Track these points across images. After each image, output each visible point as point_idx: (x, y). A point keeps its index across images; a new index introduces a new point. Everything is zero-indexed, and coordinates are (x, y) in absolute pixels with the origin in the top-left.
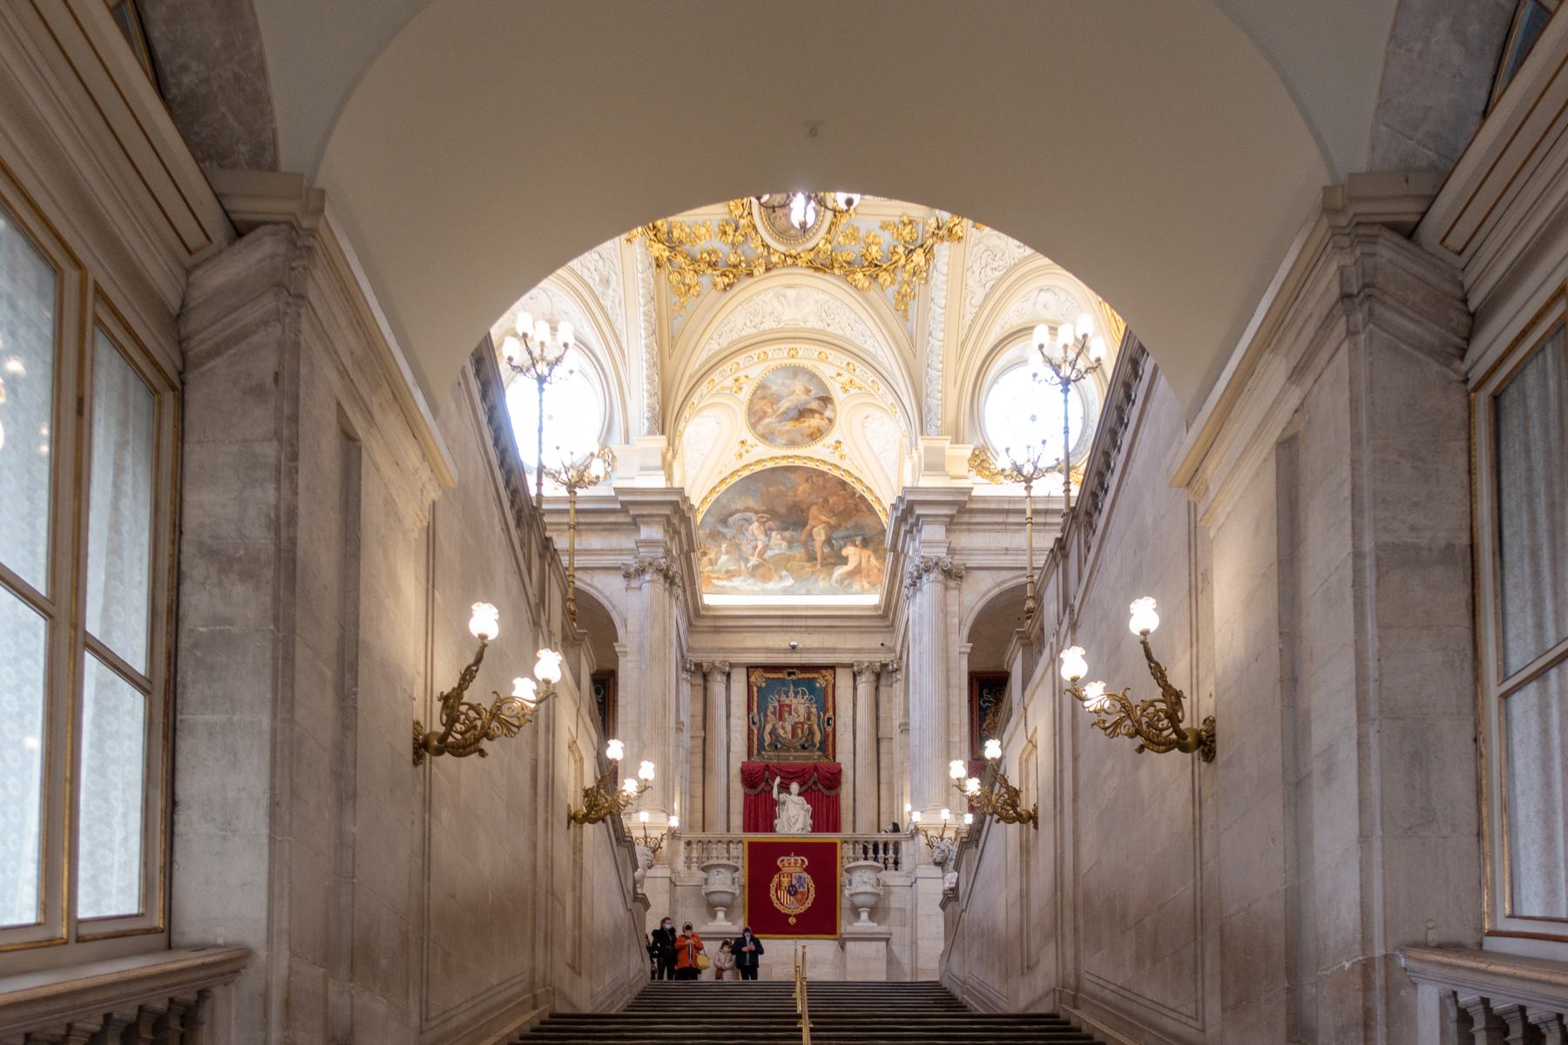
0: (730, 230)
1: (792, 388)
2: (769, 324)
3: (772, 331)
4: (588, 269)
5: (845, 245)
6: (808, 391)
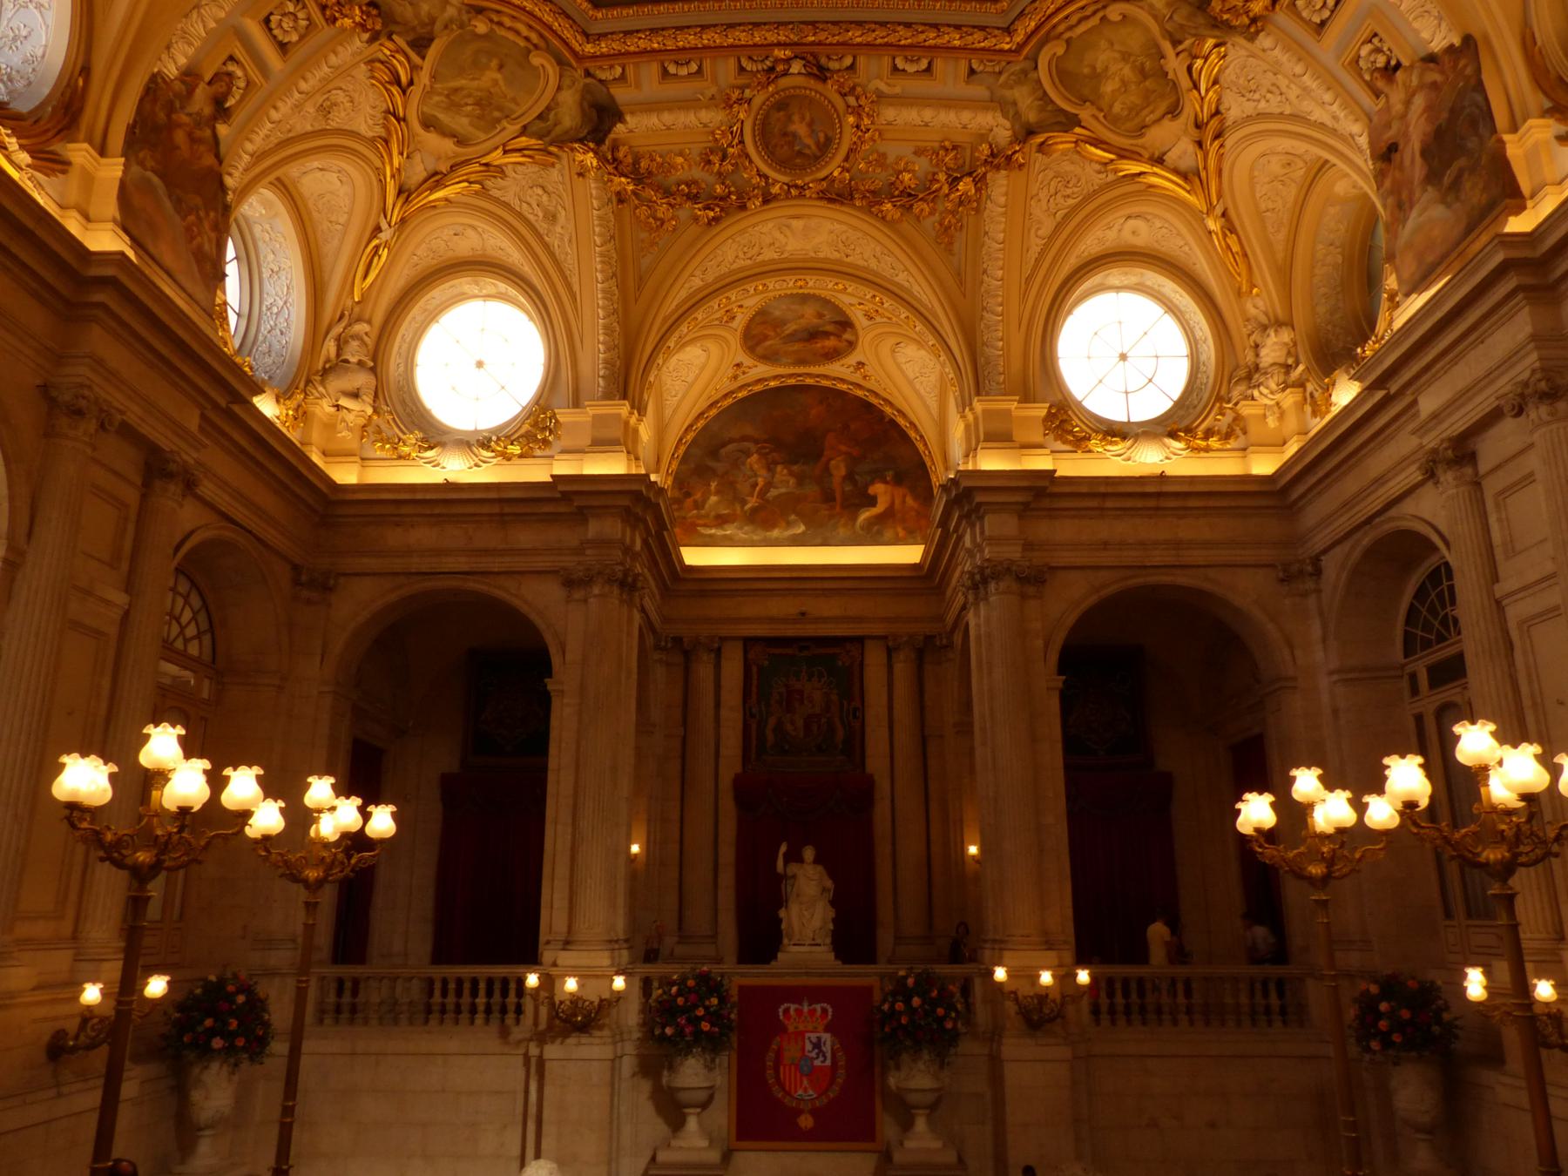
0: (715, 159)
2: (769, 255)
3: (773, 261)
4: (528, 204)
5: (867, 172)
6: (820, 316)
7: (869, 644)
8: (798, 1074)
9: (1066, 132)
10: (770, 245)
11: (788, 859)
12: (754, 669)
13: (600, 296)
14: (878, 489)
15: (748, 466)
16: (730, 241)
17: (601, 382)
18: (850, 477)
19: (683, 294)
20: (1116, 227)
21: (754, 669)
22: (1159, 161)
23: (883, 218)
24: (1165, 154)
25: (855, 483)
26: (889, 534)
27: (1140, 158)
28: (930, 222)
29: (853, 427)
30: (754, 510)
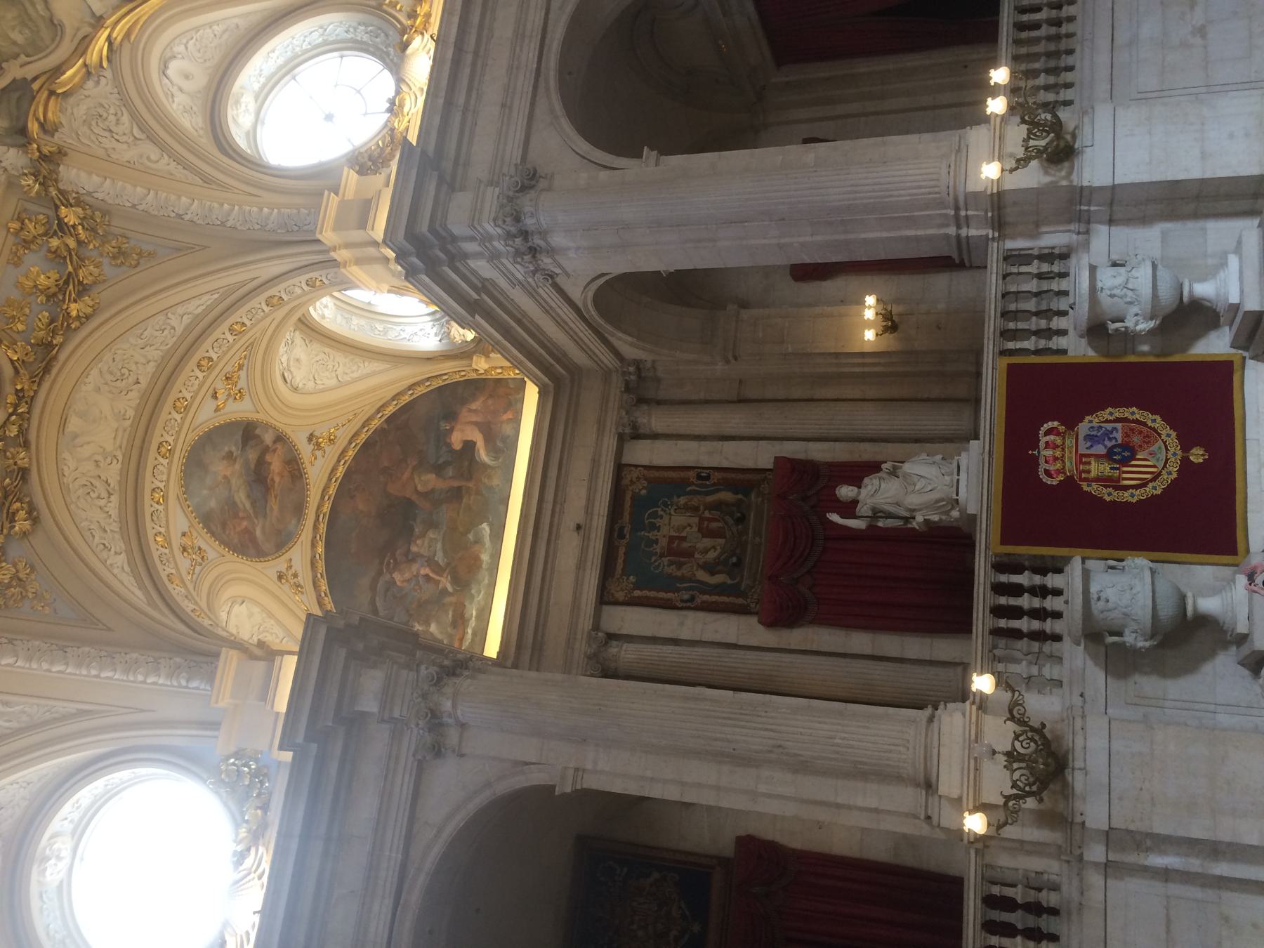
1: (220, 478)
3: (124, 473)
6: (230, 457)
7: (626, 460)
8: (1134, 463)
9: (34, 98)
10: (98, 466)
11: (853, 516)
12: (637, 593)
13: (84, 672)
14: (457, 440)
15: (405, 584)
16: (73, 507)
17: (194, 684)
18: (438, 469)
19: (129, 580)
20: (174, 90)
21: (637, 593)
22: (98, 22)
23: (88, 317)
24: (93, 14)
25: (447, 463)
26: (507, 429)
27: (87, 40)
28: (108, 269)
29: (386, 464)
30: (456, 580)
